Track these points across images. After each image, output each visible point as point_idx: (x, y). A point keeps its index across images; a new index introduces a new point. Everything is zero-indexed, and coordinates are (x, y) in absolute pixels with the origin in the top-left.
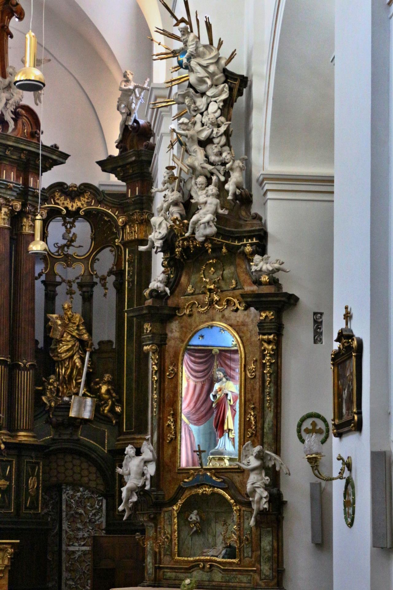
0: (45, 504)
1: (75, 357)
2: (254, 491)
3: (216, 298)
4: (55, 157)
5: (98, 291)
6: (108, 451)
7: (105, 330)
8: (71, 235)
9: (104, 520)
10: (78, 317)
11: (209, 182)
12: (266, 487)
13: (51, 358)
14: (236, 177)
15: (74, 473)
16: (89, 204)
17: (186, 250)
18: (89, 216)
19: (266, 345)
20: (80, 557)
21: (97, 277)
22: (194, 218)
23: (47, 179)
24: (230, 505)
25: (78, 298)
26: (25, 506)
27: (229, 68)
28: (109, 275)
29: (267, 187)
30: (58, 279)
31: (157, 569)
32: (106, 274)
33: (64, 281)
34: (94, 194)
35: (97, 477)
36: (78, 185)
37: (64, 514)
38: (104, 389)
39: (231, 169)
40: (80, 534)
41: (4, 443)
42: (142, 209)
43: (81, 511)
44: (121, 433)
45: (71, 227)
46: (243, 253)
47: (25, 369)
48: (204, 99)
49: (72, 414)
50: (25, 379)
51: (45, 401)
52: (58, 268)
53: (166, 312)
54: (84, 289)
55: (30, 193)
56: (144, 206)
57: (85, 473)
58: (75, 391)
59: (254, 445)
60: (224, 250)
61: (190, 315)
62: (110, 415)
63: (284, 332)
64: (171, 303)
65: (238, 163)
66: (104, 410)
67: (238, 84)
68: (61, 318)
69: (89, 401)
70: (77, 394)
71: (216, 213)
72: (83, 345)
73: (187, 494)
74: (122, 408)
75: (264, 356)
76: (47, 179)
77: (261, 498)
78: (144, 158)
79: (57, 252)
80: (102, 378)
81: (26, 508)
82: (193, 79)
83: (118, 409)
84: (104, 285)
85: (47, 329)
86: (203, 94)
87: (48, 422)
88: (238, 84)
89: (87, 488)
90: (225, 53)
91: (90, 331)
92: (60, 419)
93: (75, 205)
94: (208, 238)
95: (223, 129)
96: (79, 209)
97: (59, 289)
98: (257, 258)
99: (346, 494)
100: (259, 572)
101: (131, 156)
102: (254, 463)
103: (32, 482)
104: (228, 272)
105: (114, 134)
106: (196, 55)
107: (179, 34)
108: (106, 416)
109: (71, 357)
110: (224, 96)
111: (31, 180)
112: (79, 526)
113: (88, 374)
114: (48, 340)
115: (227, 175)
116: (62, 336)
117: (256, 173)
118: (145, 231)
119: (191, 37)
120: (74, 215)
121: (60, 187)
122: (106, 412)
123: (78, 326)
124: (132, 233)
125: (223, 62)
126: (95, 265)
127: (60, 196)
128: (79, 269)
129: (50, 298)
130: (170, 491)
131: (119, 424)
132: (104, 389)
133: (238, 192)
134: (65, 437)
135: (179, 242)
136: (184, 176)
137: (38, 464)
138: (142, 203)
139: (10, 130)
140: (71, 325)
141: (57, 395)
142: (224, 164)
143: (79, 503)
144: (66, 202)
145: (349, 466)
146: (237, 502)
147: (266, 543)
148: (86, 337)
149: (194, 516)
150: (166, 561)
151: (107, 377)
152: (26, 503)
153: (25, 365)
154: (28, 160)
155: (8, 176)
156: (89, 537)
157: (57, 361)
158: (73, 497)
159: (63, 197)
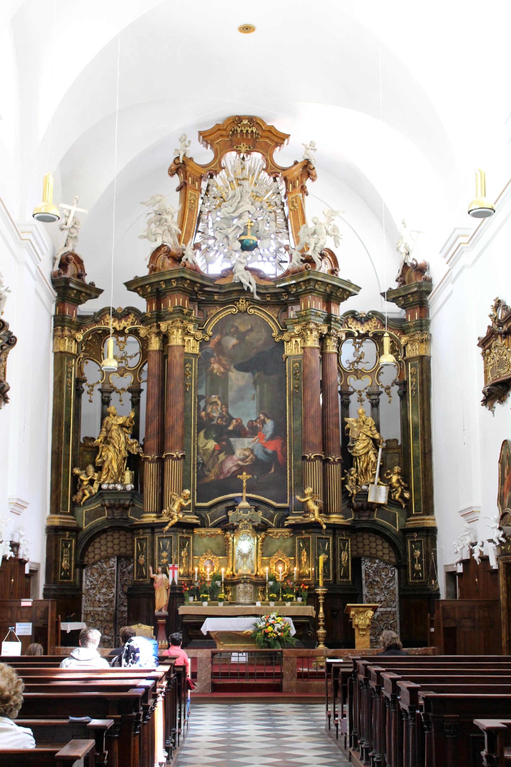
1: (370, 453)
5: (383, 398)
6: (400, 530)
7: (391, 430)
8: (360, 353)
9: (396, 586)
10: (370, 421)
13: (350, 454)
15: (371, 548)
16: (376, 327)
20: (378, 616)
21: (382, 387)
25: (367, 403)
26: (340, 576)
28: (393, 386)
30: (351, 390)
32: (390, 385)
33: (355, 391)
34: (380, 320)
35: (390, 551)
36: (366, 313)
37: (364, 582)
38: (395, 478)
40: (378, 598)
41: (325, 524)
42: (421, 330)
43: (377, 579)
44: (410, 514)
45: (359, 347)
47: (334, 462)
49: (370, 499)
50: (335, 470)
51: (349, 489)
52: (352, 381)
54: (373, 397)
55: (333, 319)
56: (424, 328)
57: (380, 547)
58: (372, 481)
62: (400, 500)
66: (395, 496)
68: (357, 422)
70: (373, 483)
74: (411, 494)
76: (345, 307)
78: (424, 289)
79: (349, 367)
80: (392, 471)
81: (341, 577)
83: (407, 495)
84: (389, 394)
87: (350, 506)
89: (381, 560)
91: (378, 430)
92: (360, 504)
93: (364, 328)
96: (368, 331)
101: (413, 288)
105: (395, 271)
108: (397, 501)
109: (367, 453)
111: (333, 308)
112: (376, 591)
113: (381, 467)
116: (359, 436)
118: (425, 349)
120: (364, 337)
121: (353, 315)
122: (397, 497)
123: (371, 427)
124: (413, 351)
126: (381, 378)
127: (353, 322)
128: (365, 383)
129: (346, 405)
131: (409, 508)
132: (395, 478)
134: (364, 519)
137: (347, 540)
138: (421, 326)
139: (317, 268)
140: (365, 426)
141: (357, 484)
143: (377, 572)
144: (357, 326)
148: (377, 436)
151: (397, 469)
152: (340, 573)
153: (334, 460)
154: (331, 292)
156: (385, 601)
157: (356, 457)
158: (371, 567)
159: (355, 322)
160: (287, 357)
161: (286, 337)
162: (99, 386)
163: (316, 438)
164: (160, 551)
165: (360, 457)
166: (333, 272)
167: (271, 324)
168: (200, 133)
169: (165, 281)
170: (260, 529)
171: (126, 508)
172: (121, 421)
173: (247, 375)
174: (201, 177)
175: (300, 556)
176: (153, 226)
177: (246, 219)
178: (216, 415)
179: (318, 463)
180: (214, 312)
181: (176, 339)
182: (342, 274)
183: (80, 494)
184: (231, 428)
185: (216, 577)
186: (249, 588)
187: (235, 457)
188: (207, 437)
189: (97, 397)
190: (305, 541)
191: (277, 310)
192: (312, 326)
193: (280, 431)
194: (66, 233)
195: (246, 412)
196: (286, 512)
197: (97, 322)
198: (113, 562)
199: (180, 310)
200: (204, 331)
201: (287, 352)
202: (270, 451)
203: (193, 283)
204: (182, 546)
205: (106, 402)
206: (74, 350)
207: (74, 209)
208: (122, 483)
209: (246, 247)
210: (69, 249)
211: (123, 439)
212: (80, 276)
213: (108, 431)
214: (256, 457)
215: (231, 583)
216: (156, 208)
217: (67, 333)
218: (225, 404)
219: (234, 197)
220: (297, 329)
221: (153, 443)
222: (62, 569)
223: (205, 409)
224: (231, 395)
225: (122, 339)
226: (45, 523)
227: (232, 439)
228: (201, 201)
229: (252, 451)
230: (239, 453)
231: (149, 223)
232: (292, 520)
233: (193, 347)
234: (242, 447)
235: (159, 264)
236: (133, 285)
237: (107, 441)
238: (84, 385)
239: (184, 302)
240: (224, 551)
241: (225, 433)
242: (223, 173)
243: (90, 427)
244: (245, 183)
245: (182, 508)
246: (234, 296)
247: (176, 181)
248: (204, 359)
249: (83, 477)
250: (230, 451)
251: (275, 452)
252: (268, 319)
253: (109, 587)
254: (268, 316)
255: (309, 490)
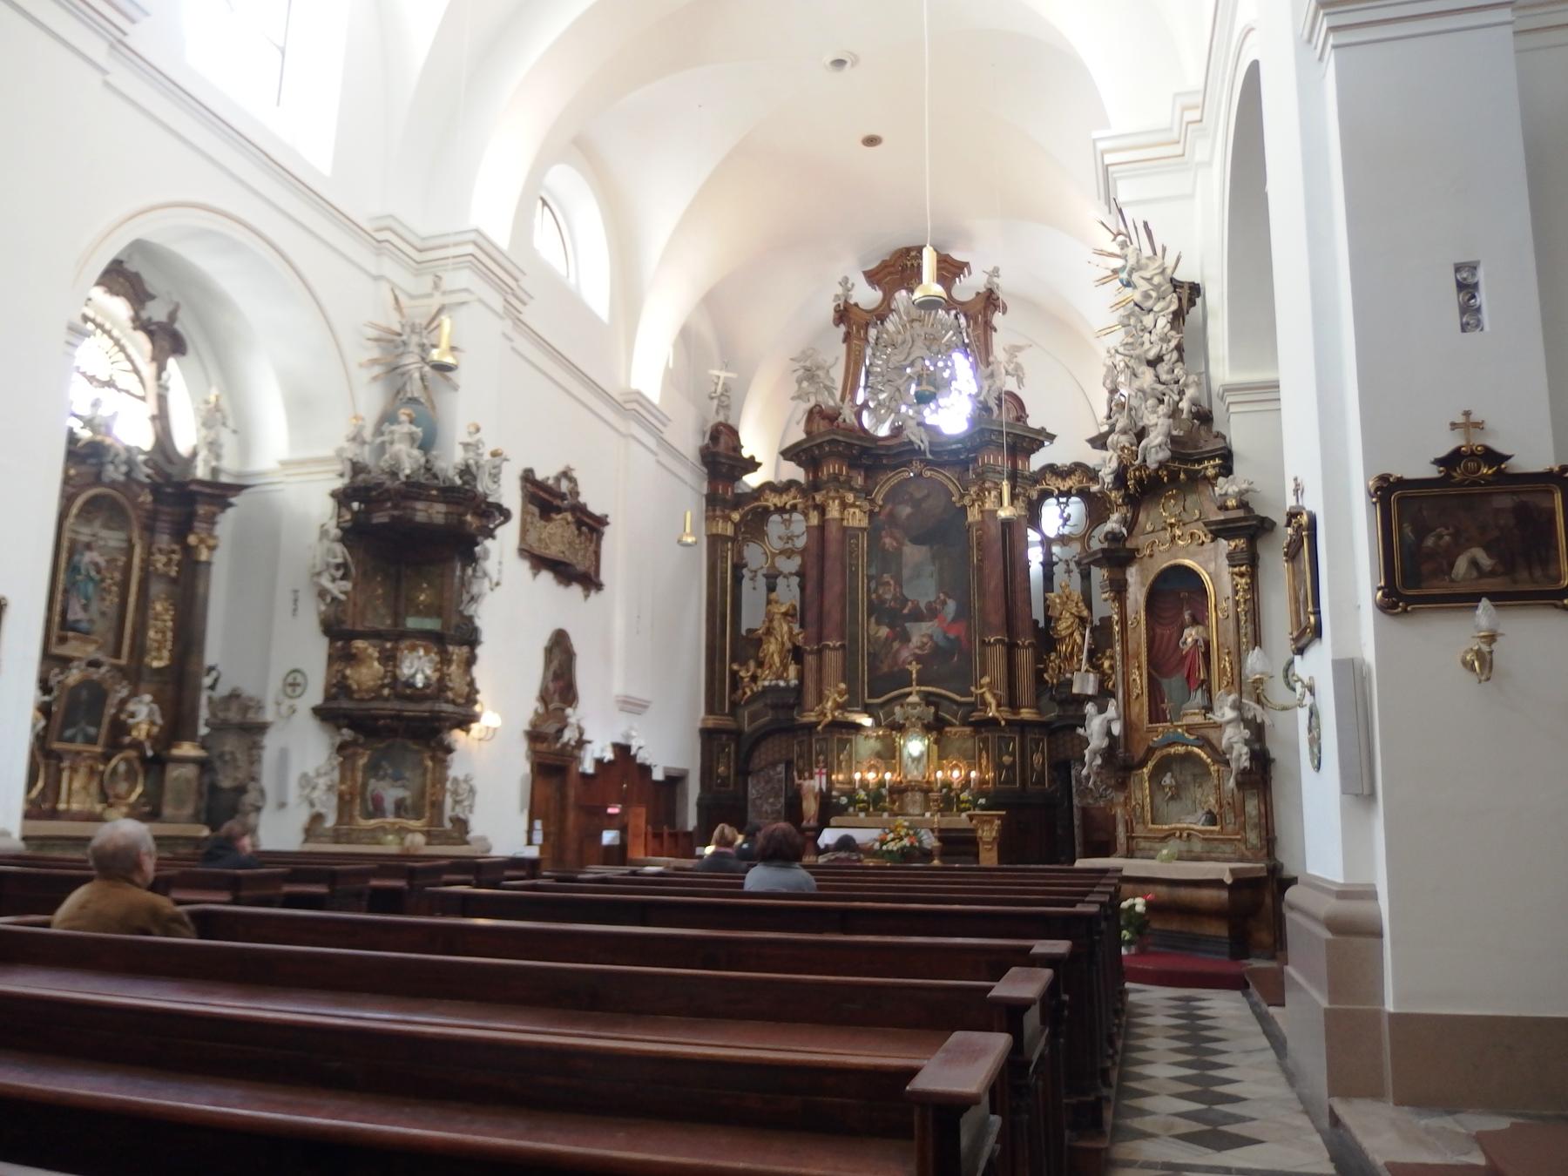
0: (1052, 781)
2: (1231, 747)
3: (1178, 532)
4: (1039, 439)
11: (1161, 402)
12: (1247, 742)
14: (1190, 392)
17: (1139, 481)
18: (1083, 494)
19: (1238, 579)
22: (1143, 443)
23: (1037, 461)
24: (1207, 766)
25: (1076, 576)
27: (1179, 276)
29: (1229, 400)
31: (1130, 838)
39: (1186, 385)
46: (1206, 478)
47: (1024, 647)
48: (1151, 315)
49: (1075, 690)
50: (1025, 657)
52: (1056, 549)
53: (1123, 554)
59: (1229, 693)
60: (1182, 476)
61: (1151, 556)
63: (1261, 563)
64: (1128, 545)
65: (1192, 378)
67: (1192, 292)
69: (1091, 676)
71: (1169, 434)
72: (1083, 621)
73: (1158, 754)
75: (1236, 593)
76: (1037, 461)
77: (1241, 756)
82: (1137, 296)
85: (1047, 608)
86: (1150, 310)
87: (1052, 698)
88: (1192, 292)
90: (1170, 261)
91: (1089, 607)
94: (1162, 465)
95: (1173, 344)
97: (1055, 568)
98: (1221, 480)
99: (1310, 731)
100: (1245, 841)
102: (1230, 714)
103: (1037, 759)
104: (1191, 500)
106: (1138, 267)
107: (1117, 250)
110: (1174, 307)
113: (1089, 651)
114: (1048, 619)
115: (1181, 393)
117: (1216, 386)
119: (1130, 251)
121: (1051, 469)
125: (1169, 271)
130: (1140, 753)
133: (1194, 409)
135: (1131, 474)
136: (1134, 402)
142: (1177, 382)
145: (1311, 690)
146: (1215, 762)
147: (1252, 807)
148: (1085, 613)
149: (1168, 780)
150: (1139, 830)
155: (996, 459)
160: (970, 526)
161: (967, 501)
162: (764, 571)
163: (996, 618)
164: (818, 755)
165: (1062, 639)
166: (1018, 419)
167: (951, 487)
168: (865, 273)
169: (820, 446)
170: (927, 728)
171: (792, 707)
172: (783, 609)
173: (924, 549)
174: (867, 325)
175: (980, 757)
176: (805, 384)
177: (918, 367)
178: (888, 596)
179: (1000, 649)
180: (885, 478)
181: (834, 511)
182: (1034, 422)
183: (740, 692)
184: (906, 611)
185: (881, 784)
186: (918, 796)
187: (911, 645)
188: (878, 623)
189: (761, 582)
190: (985, 741)
191: (958, 469)
192: (987, 485)
193: (964, 612)
194: (716, 402)
195: (923, 591)
196: (972, 707)
197: (757, 499)
198: (781, 768)
199: (835, 478)
200: (872, 501)
201: (970, 519)
202: (952, 636)
203: (850, 446)
204: (840, 751)
205: (771, 588)
206: (730, 531)
207: (723, 374)
208: (787, 680)
209: (923, 399)
210: (721, 418)
211: (785, 628)
212: (737, 447)
213: (771, 621)
214: (936, 644)
215: (898, 791)
216: (808, 364)
217: (718, 513)
218: (899, 583)
219: (904, 342)
220: (973, 490)
221: (812, 630)
222: (718, 776)
223: (876, 591)
224: (906, 573)
225: (786, 516)
226: (699, 725)
227: (907, 625)
228: (869, 351)
229: (931, 637)
230: (915, 640)
231: (799, 382)
232: (976, 715)
233: (857, 518)
234: (921, 633)
235: (815, 428)
236: (790, 454)
237: (769, 632)
238: (745, 571)
239: (841, 469)
240: (889, 755)
241: (897, 617)
242: (893, 317)
243: (752, 619)
244: (916, 324)
245: (838, 706)
246: (906, 458)
247: (843, 328)
248: (874, 532)
249: (742, 674)
250: (906, 638)
251: (958, 638)
252: (946, 482)
253: (777, 796)
254: (946, 477)
255: (986, 680)
